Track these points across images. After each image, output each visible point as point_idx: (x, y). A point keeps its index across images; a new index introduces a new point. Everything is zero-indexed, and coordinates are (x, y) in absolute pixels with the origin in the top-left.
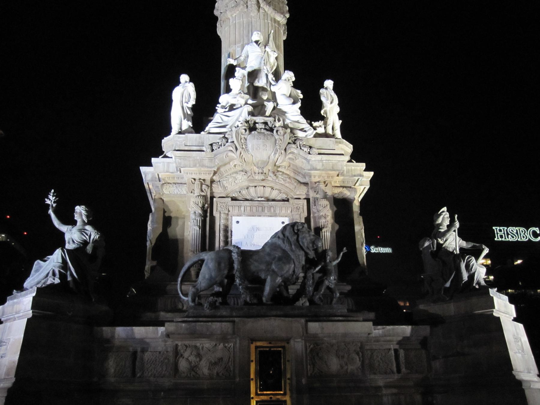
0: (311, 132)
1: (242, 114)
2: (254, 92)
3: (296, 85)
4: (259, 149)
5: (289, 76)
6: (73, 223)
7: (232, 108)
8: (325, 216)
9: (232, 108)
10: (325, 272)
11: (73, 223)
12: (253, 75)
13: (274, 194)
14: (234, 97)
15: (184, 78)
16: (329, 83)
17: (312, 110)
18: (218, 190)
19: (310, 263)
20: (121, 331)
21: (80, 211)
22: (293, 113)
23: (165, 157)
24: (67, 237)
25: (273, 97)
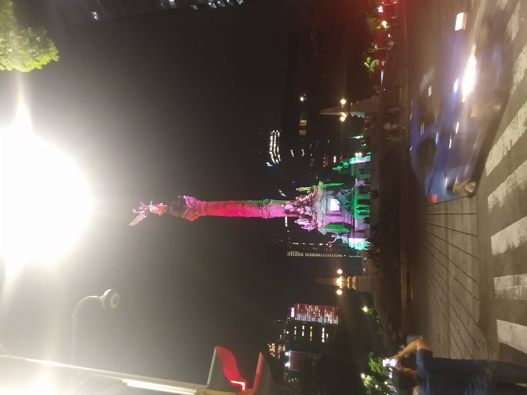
0: (312, 193)
1: (308, 208)
2: (298, 207)
3: (299, 196)
4: (317, 204)
5: (297, 198)
6: (334, 238)
7: (305, 211)
8: (331, 192)
9: (305, 211)
10: (345, 192)
11: (334, 238)
12: (294, 206)
13: (326, 202)
14: (301, 211)
15: (296, 222)
16: (297, 189)
17: (305, 193)
18: (325, 213)
19: (343, 194)
20: (356, 226)
21: (333, 236)
22: (307, 197)
23: (317, 225)
24: (338, 238)
25: (303, 201)
